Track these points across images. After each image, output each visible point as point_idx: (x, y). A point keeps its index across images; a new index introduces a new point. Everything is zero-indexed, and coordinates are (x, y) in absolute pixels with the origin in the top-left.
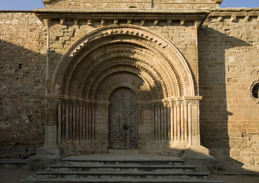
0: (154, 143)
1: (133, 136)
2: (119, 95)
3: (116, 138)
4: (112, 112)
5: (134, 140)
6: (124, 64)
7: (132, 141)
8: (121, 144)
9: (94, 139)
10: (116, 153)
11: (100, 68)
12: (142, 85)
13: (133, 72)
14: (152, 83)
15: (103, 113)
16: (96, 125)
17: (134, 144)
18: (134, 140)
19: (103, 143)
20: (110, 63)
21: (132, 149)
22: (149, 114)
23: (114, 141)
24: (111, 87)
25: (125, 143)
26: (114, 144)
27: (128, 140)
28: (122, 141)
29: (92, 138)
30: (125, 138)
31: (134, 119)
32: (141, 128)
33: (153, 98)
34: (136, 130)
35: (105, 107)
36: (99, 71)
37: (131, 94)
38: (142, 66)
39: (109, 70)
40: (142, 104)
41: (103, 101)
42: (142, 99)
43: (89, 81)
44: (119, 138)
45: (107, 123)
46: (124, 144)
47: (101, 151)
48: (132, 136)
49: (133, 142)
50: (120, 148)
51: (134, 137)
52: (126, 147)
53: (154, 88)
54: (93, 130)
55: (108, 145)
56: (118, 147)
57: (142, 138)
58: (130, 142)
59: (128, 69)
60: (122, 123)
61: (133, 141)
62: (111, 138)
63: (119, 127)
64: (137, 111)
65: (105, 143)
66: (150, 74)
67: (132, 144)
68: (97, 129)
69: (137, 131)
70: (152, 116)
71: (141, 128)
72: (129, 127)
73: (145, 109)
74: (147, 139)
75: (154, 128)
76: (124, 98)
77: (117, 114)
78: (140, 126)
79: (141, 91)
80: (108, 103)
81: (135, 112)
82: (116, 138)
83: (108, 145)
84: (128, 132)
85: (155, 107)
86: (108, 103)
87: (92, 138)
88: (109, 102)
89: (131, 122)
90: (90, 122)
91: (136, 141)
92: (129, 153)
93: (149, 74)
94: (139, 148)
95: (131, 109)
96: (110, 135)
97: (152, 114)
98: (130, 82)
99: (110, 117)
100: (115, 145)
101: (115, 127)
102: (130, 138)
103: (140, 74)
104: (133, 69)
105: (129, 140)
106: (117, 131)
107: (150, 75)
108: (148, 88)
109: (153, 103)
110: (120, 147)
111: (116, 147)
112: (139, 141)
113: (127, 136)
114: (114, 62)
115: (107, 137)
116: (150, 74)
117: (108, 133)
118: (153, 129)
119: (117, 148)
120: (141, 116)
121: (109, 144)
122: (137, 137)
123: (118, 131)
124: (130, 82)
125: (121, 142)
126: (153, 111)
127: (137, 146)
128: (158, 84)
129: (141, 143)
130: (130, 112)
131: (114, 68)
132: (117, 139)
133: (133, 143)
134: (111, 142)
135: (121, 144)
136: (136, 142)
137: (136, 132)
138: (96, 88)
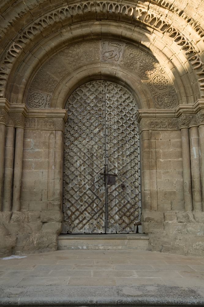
0: (191, 218)
1: (129, 199)
2: (89, 95)
3: (82, 205)
4: (72, 139)
5: (132, 210)
6: (105, 11)
7: (125, 215)
8: (95, 222)
9: (20, 209)
10: (83, 249)
11: (39, 20)
12: (152, 68)
13: (127, 33)
14: (181, 60)
15: (47, 140)
16: (27, 171)
17: (132, 222)
18: (132, 210)
19: (45, 220)
20: (66, 7)
21: (128, 236)
22: (173, 141)
23: (77, 213)
24: (69, 74)
25: (107, 218)
26: (77, 221)
27: (114, 212)
28: (97, 215)
29: (12, 205)
30: (107, 205)
31: (130, 155)
32: (151, 178)
33: (184, 98)
34: (137, 184)
35: (54, 123)
36: (37, 27)
37: (121, 93)
38: (152, 15)
39: (65, 30)
40: (152, 117)
41: (49, 107)
42: (152, 104)
43: (9, 53)
44: (89, 206)
45: (58, 166)
46: (103, 223)
47: (38, 244)
48: (126, 202)
49: (129, 217)
50: (92, 234)
51: (131, 204)
53: (186, 73)
54: (17, 184)
55: (60, 224)
56: (87, 231)
57: (155, 204)
58: (121, 218)
59: (114, 28)
60: (99, 166)
61: (128, 214)
63: (90, 177)
64: (138, 137)
66: (176, 35)
67: (127, 221)
68: (29, 180)
69: (139, 189)
70: (181, 147)
71: (151, 178)
73: (160, 127)
74: (170, 209)
75: (189, 179)
76: (103, 103)
77: (83, 145)
78: (147, 172)
79: (149, 85)
80: (60, 115)
81: (134, 137)
82: (82, 205)
83: (58, 226)
84: (115, 189)
85: (190, 122)
86: (60, 115)
87: (12, 205)
88: (64, 111)
89: (123, 164)
90: (9, 163)
91: (136, 213)
92: (120, 247)
93: (172, 36)
95: (121, 131)
96: (66, 197)
97: (181, 142)
98: (118, 62)
99: (67, 150)
100: (78, 224)
101: (79, 178)
102: (120, 205)
103: (148, 40)
104: (128, 26)
105: (118, 211)
106: (85, 189)
107: (177, 37)
108: (169, 76)
109: (184, 112)
110: (93, 230)
111: (82, 231)
112: (147, 214)
113: (112, 201)
114: (78, 5)
115: (57, 203)
116: (176, 35)
117: (58, 191)
118: (187, 181)
120: (150, 146)
121: (63, 221)
122: (139, 204)
123: (87, 187)
124: (119, 61)
125: (95, 217)
126: (185, 132)
127: (139, 226)
128: (198, 60)
129: (153, 219)
130: (120, 138)
131: (78, 25)
132: (85, 210)
133: (130, 219)
134: (69, 217)
135: (95, 222)
136: (137, 217)
138: (27, 74)
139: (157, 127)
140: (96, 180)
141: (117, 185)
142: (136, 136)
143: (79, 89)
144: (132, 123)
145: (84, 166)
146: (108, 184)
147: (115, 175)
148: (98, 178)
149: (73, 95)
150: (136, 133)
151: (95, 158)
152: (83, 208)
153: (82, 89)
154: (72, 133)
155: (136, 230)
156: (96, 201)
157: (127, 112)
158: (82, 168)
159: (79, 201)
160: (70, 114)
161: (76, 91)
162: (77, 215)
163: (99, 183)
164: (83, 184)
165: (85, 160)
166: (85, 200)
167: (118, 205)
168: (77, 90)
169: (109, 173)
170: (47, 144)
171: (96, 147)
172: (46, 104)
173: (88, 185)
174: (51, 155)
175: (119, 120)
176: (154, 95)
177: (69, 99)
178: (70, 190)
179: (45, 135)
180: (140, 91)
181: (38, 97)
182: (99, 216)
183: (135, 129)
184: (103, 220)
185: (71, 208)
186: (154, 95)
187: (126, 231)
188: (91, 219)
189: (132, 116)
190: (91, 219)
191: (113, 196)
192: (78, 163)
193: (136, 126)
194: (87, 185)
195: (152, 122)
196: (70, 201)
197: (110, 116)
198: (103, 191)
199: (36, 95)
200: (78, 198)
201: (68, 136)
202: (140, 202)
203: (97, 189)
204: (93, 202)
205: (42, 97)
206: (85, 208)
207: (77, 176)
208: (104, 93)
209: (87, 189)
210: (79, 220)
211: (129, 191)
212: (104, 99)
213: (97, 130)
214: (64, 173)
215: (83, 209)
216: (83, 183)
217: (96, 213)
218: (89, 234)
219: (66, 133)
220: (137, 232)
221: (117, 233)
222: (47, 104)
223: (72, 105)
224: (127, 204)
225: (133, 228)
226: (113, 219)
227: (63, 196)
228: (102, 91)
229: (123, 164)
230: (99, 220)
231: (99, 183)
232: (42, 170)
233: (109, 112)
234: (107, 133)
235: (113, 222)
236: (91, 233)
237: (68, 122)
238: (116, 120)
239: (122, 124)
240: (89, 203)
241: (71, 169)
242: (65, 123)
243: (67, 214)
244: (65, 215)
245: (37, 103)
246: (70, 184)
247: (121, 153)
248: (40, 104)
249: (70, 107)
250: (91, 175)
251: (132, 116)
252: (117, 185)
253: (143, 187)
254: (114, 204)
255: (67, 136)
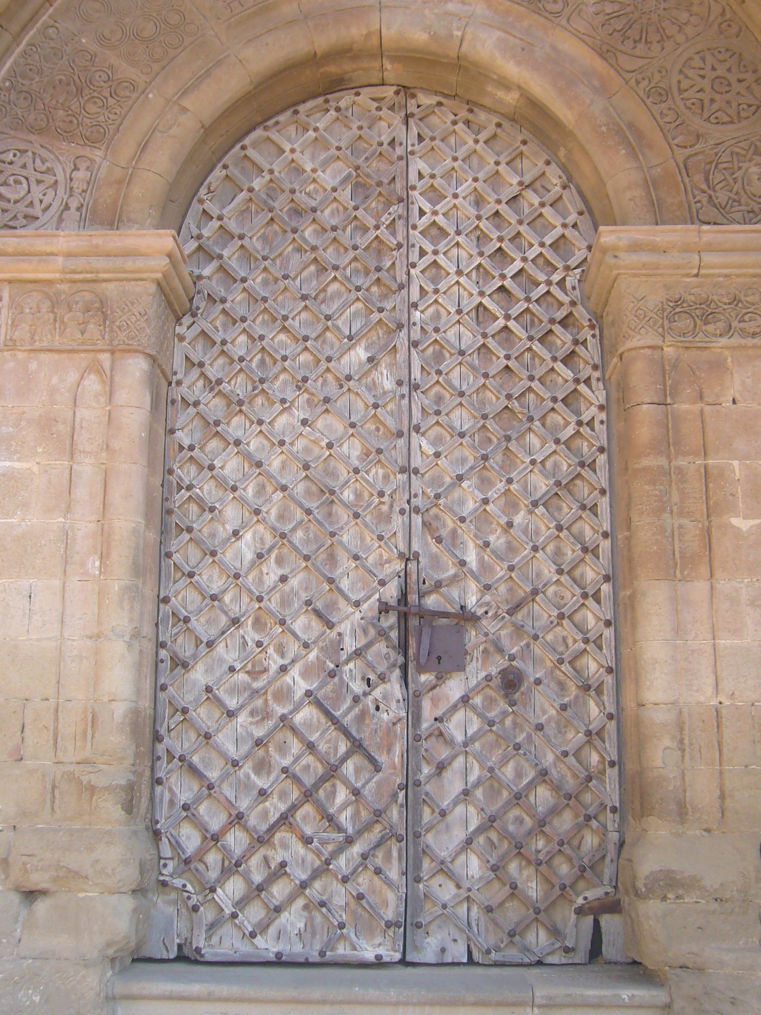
18: (565, 822)
23: (236, 840)
25: (412, 874)
26: (234, 887)
27: (459, 835)
28: (357, 849)
32: (678, 630)
35: (102, 310)
44: (308, 795)
45: (121, 557)
46: (391, 897)
52: (429, 947)
55: (128, 903)
57: (702, 790)
62: (183, 789)
63: (317, 626)
65: (71, 877)
67: (533, 889)
72: (474, 619)
78: (655, 600)
82: (262, 793)
84: (465, 700)
86: (140, 263)
94: (636, 970)
106: (283, 695)
110: (330, 945)
111: (266, 945)
113: (441, 768)
117: (120, 710)
119: (279, 962)
120: (669, 440)
121: (148, 886)
122: (610, 789)
123: (298, 682)
125: (342, 863)
127: (606, 920)
132: (285, 819)
135: (340, 895)
137: (594, 709)
139: (710, 328)
140: (350, 645)
141: (476, 671)
142: (582, 388)
143: (259, 133)
144: (560, 314)
145: (280, 561)
146: (421, 669)
147: (466, 617)
148: (365, 632)
149: (225, 167)
150: (587, 372)
151: (343, 515)
152: (276, 807)
153: (274, 135)
154: (213, 372)
155: (585, 944)
156: (349, 768)
157: (531, 254)
158: (271, 572)
159: (247, 768)
160: (206, 272)
161: (243, 148)
162: (238, 852)
163: (370, 666)
164: (274, 668)
165: (287, 528)
166: (286, 762)
167: (479, 793)
168: (247, 141)
169: (432, 601)
170: (63, 429)
171: (352, 449)
172: (67, 207)
173: (305, 674)
174: (81, 492)
175: (486, 301)
176: (688, 151)
177: (203, 191)
178: (198, 703)
179: (55, 380)
180: (604, 129)
181: (24, 172)
182: (364, 856)
183: (580, 349)
184: (389, 883)
185: (203, 809)
186: (688, 151)
187: (526, 949)
188: (316, 874)
189: (564, 279)
190: (316, 874)
191: (450, 742)
192: (246, 547)
193: (586, 334)
194: (295, 672)
195: (679, 302)
196: (193, 770)
197: (435, 280)
198: (394, 711)
199: (11, 163)
200: (245, 748)
201: (192, 387)
202: (612, 774)
203: (356, 700)
204: (332, 772)
205: (44, 169)
206: (283, 807)
207: (235, 622)
208: (399, 151)
209: (299, 694)
210: (248, 881)
211: (543, 705)
212: (399, 185)
213: (361, 353)
214: (166, 600)
215: (274, 817)
216: (274, 662)
217: (350, 841)
218: (307, 964)
219: (179, 376)
220: (595, 951)
221: (471, 962)
222: (74, 204)
223: (220, 218)
224: (532, 785)
225: (569, 930)
226: (450, 875)
227: (157, 738)
228: (392, 143)
229: (511, 549)
230: (364, 881)
231: (370, 666)
232: (25, 583)
233: (428, 259)
234: (417, 374)
235: (446, 891)
236: (315, 957)
237: (194, 315)
238: (468, 305)
239: (501, 322)
240: (308, 781)
241: (202, 579)
242: (178, 320)
243: (176, 846)
244: (167, 851)
245: (16, 202)
246: (200, 667)
247: (501, 486)
248: (30, 211)
249: (206, 233)
250: (318, 614)
251: (564, 279)
252: (476, 671)
253: (629, 688)
254: (458, 787)
255: (184, 389)
